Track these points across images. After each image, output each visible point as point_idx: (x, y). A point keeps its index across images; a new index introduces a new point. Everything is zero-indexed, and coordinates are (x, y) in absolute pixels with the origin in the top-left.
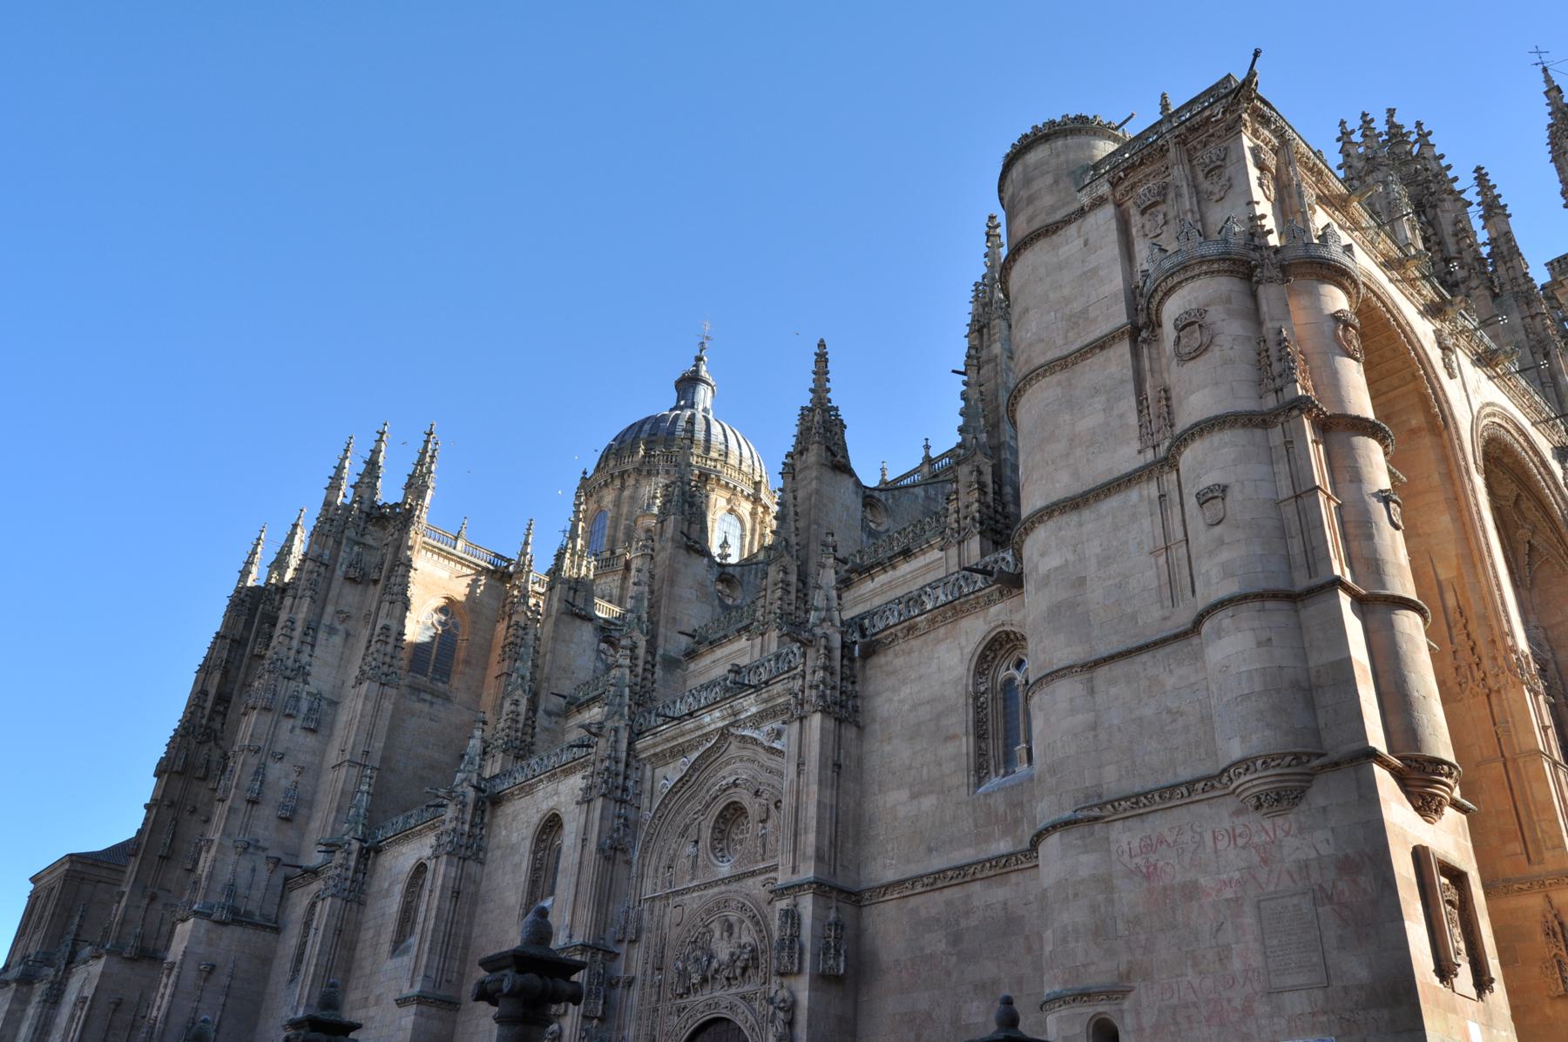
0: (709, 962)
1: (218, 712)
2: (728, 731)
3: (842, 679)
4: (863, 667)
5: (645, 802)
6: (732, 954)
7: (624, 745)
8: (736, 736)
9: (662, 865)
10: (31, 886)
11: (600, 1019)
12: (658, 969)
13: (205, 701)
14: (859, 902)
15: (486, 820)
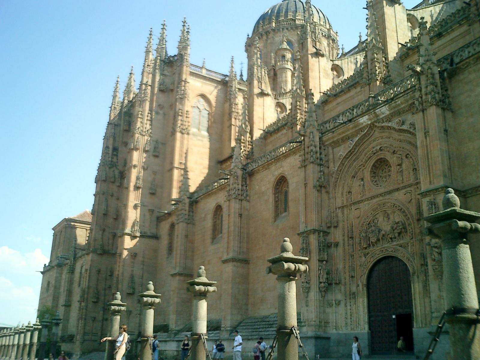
0: (379, 232)
1: (115, 155)
2: (373, 125)
3: (442, 89)
4: (450, 82)
5: (331, 165)
6: (392, 227)
7: (317, 139)
8: (378, 127)
9: (345, 191)
10: (53, 232)
11: (327, 261)
12: (350, 238)
13: (109, 151)
14: (465, 195)
15: (248, 183)
